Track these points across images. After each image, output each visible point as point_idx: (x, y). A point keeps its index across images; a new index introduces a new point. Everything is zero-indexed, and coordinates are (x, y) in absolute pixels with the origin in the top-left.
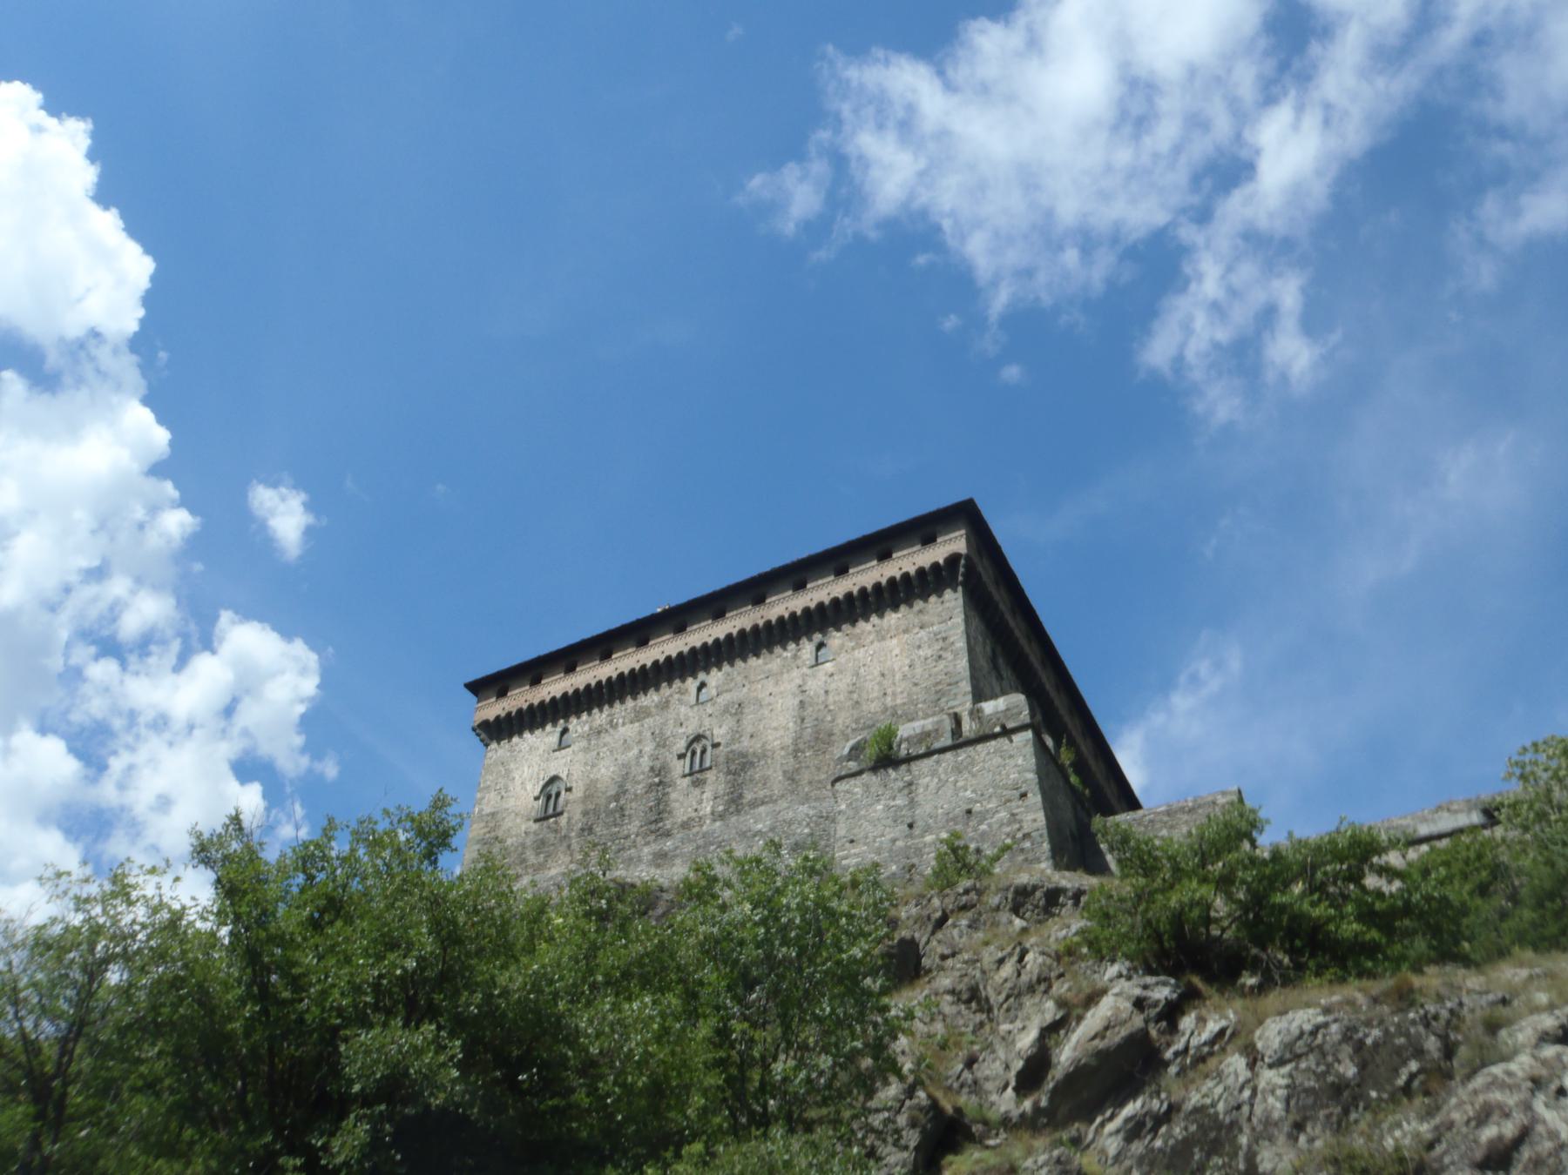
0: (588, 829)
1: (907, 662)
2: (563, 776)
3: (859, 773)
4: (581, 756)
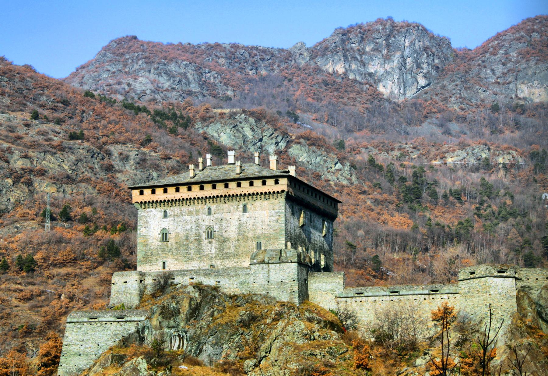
0: (177, 249)
1: (269, 220)
2: (167, 228)
3: (256, 264)
4: (172, 223)
